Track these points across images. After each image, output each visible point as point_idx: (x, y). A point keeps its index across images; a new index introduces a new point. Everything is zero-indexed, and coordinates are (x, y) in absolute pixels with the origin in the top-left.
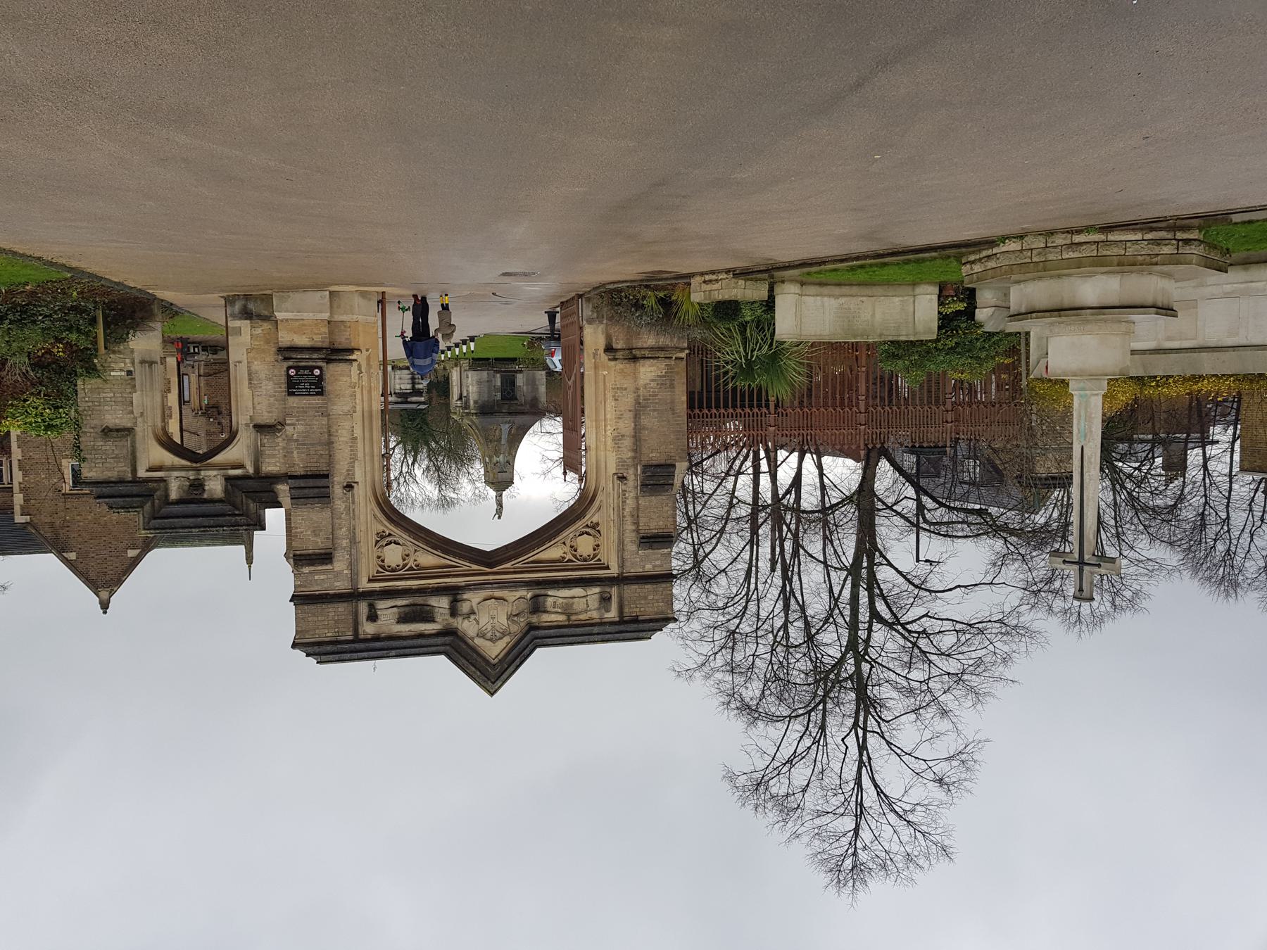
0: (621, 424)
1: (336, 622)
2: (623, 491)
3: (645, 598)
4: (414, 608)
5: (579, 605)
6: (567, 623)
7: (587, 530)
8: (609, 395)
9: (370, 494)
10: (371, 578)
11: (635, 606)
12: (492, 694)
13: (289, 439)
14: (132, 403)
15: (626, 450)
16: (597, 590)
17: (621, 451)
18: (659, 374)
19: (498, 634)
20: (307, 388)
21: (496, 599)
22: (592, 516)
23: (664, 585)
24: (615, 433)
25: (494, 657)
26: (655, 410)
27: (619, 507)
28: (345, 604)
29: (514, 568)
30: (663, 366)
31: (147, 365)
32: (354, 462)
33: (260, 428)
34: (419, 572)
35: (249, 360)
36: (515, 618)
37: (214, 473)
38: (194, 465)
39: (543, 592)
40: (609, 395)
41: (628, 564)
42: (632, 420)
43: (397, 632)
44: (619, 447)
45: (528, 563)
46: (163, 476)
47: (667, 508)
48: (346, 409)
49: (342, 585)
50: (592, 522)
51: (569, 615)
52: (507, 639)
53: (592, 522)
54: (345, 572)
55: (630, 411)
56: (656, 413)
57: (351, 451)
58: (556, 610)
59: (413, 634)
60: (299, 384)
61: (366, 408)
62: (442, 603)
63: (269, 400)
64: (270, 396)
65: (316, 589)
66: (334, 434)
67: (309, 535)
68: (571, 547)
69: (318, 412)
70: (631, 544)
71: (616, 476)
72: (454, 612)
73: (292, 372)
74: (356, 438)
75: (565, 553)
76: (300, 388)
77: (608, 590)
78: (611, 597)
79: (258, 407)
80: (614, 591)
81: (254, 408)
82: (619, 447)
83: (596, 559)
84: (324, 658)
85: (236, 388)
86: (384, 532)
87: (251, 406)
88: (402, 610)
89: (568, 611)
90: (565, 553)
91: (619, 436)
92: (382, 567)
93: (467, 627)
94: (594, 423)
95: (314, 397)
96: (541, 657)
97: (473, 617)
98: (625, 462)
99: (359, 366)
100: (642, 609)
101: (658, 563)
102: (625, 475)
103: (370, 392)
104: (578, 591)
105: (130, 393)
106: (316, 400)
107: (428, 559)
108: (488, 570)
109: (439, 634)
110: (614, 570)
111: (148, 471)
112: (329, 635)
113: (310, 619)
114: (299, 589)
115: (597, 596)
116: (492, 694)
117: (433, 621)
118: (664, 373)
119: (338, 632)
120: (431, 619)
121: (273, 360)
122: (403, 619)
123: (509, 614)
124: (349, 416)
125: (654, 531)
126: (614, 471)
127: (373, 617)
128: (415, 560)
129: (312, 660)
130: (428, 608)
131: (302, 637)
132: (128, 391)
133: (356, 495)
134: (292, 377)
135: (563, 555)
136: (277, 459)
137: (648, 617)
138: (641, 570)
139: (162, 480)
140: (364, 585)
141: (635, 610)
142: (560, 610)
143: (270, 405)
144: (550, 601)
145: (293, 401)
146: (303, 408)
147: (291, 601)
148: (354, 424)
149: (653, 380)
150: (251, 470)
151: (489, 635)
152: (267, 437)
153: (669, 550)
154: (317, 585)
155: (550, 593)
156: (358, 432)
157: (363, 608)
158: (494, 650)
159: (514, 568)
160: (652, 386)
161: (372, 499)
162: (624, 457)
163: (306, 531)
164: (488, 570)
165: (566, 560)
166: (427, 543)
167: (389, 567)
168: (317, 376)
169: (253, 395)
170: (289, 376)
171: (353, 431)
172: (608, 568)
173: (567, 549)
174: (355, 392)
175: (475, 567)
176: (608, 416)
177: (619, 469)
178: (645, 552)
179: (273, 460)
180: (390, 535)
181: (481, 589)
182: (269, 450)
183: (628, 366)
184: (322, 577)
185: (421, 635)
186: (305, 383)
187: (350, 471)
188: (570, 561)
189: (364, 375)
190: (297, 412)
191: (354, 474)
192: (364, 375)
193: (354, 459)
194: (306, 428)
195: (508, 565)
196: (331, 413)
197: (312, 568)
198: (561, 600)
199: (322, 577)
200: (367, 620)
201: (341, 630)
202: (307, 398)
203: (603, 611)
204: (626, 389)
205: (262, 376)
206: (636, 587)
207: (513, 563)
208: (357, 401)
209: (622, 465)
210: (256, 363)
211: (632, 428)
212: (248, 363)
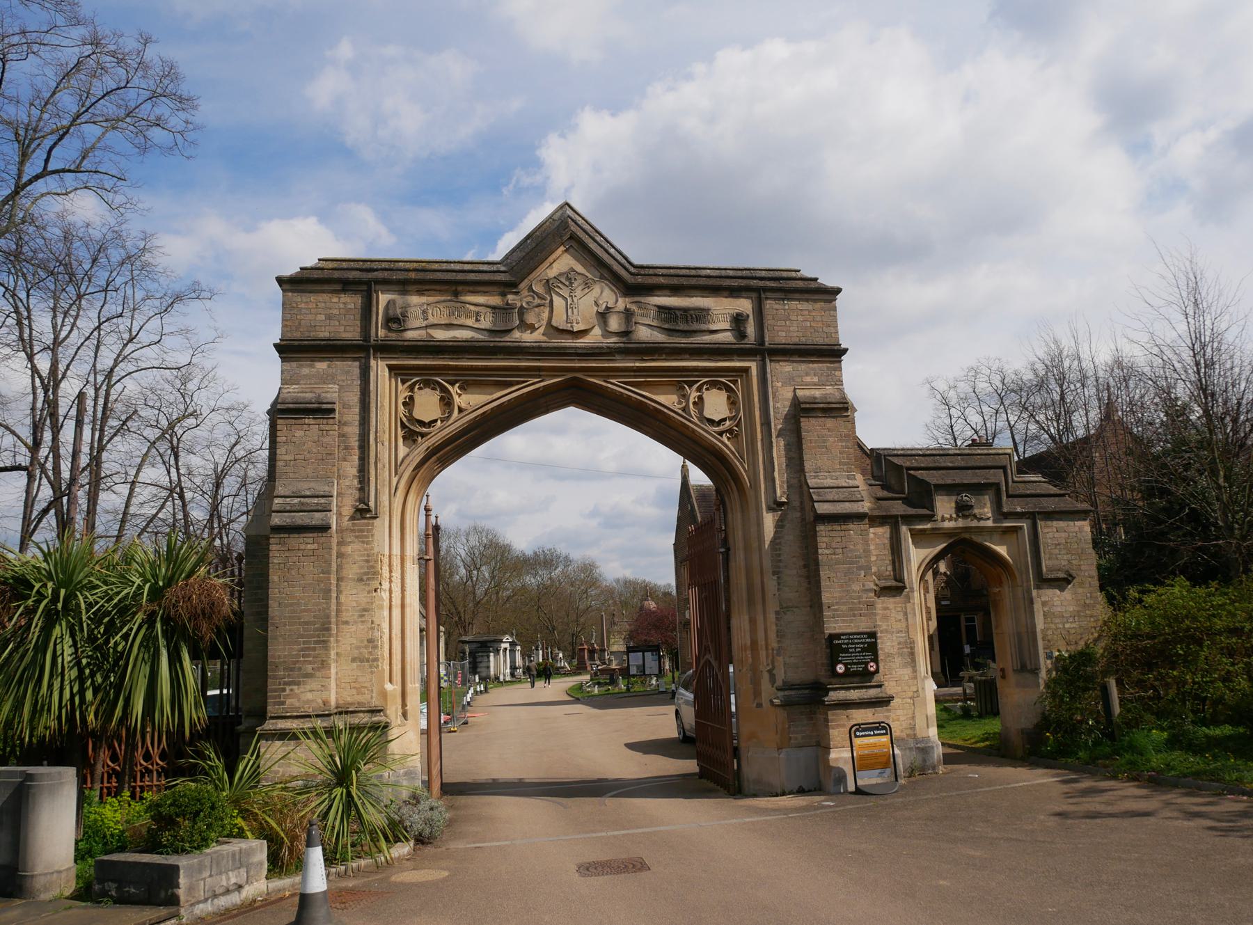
0: (363, 598)
1: (787, 318)
3: (329, 317)
4: (686, 327)
6: (460, 288)
7: (424, 430)
10: (744, 374)
11: (349, 307)
14: (1044, 615)
15: (356, 557)
16: (410, 335)
18: (295, 687)
20: (852, 644)
23: (297, 335)
24: (375, 584)
28: (777, 340)
30: (288, 701)
31: (1029, 668)
34: (680, 380)
37: (947, 524)
44: (368, 561)
47: (287, 458)
54: (779, 384)
55: (347, 623)
57: (779, 555)
58: (477, 309)
60: (864, 650)
62: (644, 334)
63: (888, 626)
64: (887, 631)
67: (831, 436)
69: (835, 610)
70: (351, 404)
74: (774, 573)
76: (862, 643)
77: (390, 334)
79: (901, 616)
80: (380, 333)
81: (906, 614)
82: (368, 561)
84: (794, 274)
88: (704, 327)
91: (368, 579)
93: (607, 295)
95: (841, 631)
97: (602, 309)
98: (357, 537)
101: (305, 371)
103: (754, 643)
105: (1048, 629)
107: (668, 400)
108: (579, 375)
109: (650, 290)
113: (820, 325)
114: (836, 365)
117: (660, 307)
118: (288, 688)
120: (661, 308)
122: (701, 314)
124: (785, 605)
125: (312, 421)
126: (376, 522)
127: (738, 321)
132: (1050, 632)
134: (872, 660)
142: (472, 308)
143: (885, 618)
147: (845, 351)
150: (904, 529)
152: (888, 573)
154: (813, 369)
156: (771, 583)
158: (562, 262)
160: (310, 667)
164: (579, 375)
165: (457, 385)
168: (840, 662)
169: (908, 632)
170: (876, 660)
171: (779, 584)
174: (779, 642)
177: (368, 525)
180: (721, 434)
183: (349, 699)
184: (808, 379)
185: (676, 290)
192: (764, 667)
194: (850, 586)
196: (809, 608)
198: (470, 322)
199: (808, 379)
200: (748, 316)
201: (780, 307)
204: (354, 660)
205: (898, 660)
208: (774, 628)
209: (362, 531)
210: (907, 677)
211: (344, 593)
212: (915, 678)
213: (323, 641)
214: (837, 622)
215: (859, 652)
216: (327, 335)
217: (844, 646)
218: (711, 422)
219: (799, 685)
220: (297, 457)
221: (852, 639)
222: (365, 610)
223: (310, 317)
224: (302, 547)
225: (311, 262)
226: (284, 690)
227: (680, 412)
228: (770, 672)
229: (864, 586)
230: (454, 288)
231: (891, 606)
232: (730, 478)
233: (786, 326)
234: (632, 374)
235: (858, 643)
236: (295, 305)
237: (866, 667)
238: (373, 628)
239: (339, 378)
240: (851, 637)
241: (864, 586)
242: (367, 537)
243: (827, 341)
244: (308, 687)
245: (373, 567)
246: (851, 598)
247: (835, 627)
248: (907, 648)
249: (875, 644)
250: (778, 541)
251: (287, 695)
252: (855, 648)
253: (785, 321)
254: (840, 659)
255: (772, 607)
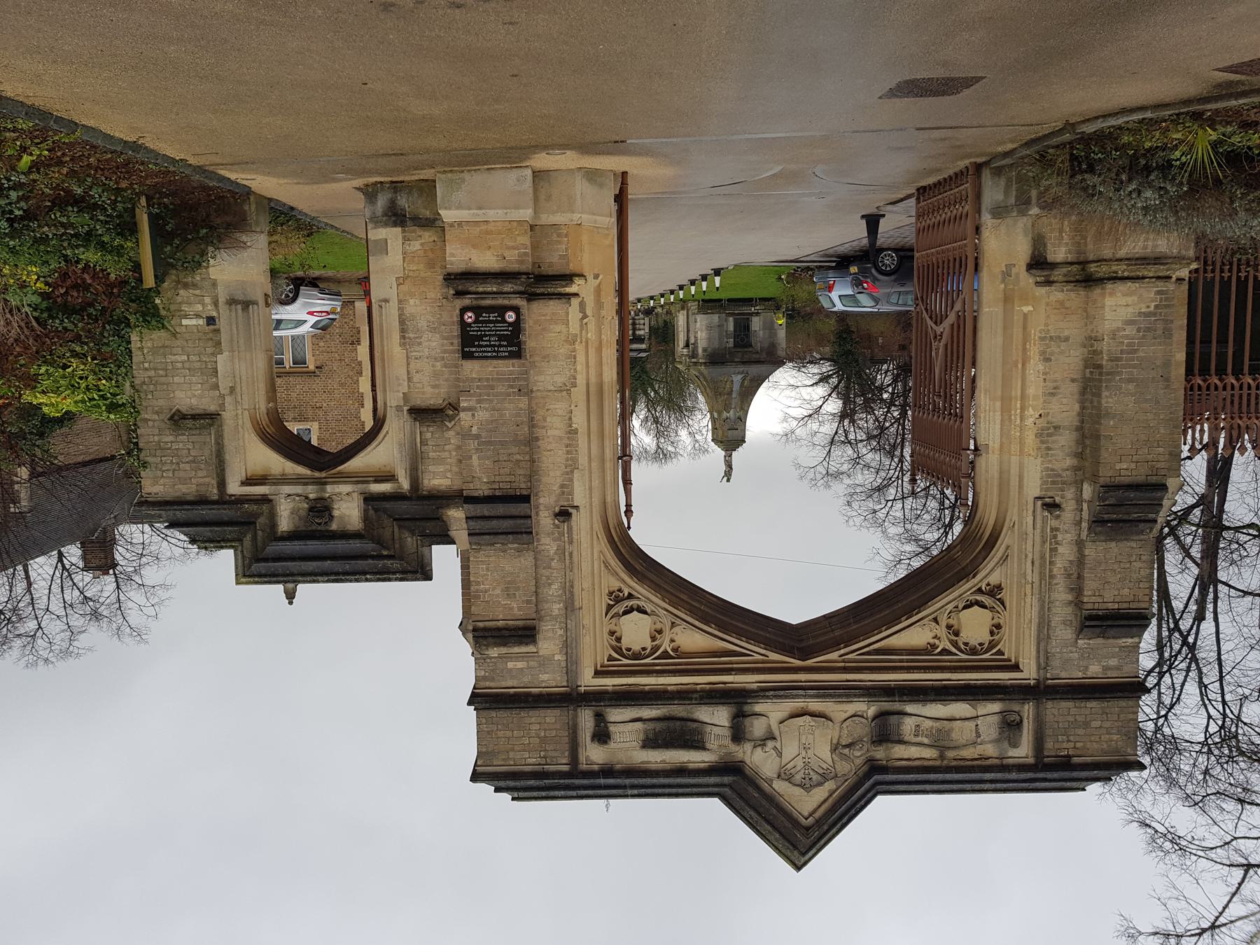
1: (543, 740)
2: (1052, 530)
3: (1086, 724)
4: (671, 724)
5: (961, 733)
6: (938, 763)
7: (979, 598)
8: (1034, 351)
9: (598, 527)
10: (599, 668)
12: (798, 868)
13: (465, 435)
14: (217, 372)
15: (1061, 454)
16: (995, 707)
17: (1052, 455)
19: (815, 777)
21: (813, 715)
22: (990, 573)
23: (1123, 703)
24: (1042, 423)
25: (806, 814)
26: (1130, 381)
27: (1042, 557)
28: (557, 712)
29: (843, 661)
31: (239, 307)
32: (572, 472)
33: (421, 414)
34: (680, 661)
35: (401, 296)
36: (846, 751)
37: (345, 488)
38: (317, 474)
39: (897, 706)
40: (1034, 351)
41: (1056, 662)
42: (1076, 397)
43: (642, 763)
44: (1048, 449)
45: (868, 653)
46: (267, 492)
47: (1138, 565)
48: (560, 380)
49: (551, 680)
50: (988, 585)
51: (942, 749)
52: (830, 785)
53: (988, 585)
55: (1073, 380)
56: (1131, 386)
57: (568, 452)
58: (919, 739)
59: (668, 767)
60: (480, 338)
61: (593, 380)
62: (717, 718)
63: (433, 366)
65: (510, 684)
66: (540, 424)
67: (497, 596)
68: (949, 627)
69: (511, 387)
70: (1062, 627)
71: (1039, 503)
72: (738, 735)
73: (469, 317)
74: (576, 432)
75: (935, 637)
78: (1021, 721)
81: (409, 379)
82: (1048, 449)
83: (994, 651)
84: (521, 794)
85: (382, 346)
86: (620, 590)
87: (406, 378)
88: (650, 726)
89: (940, 741)
90: (935, 637)
91: (1049, 429)
92: (618, 650)
93: (761, 761)
94: (998, 404)
95: (506, 361)
96: (883, 805)
98: (1060, 476)
99: (582, 306)
100: (1079, 745)
101: (1113, 662)
102: (1058, 500)
103: (599, 349)
104: (960, 708)
105: (213, 354)
106: (507, 367)
107: (693, 639)
109: (711, 770)
110: (1029, 672)
111: (243, 484)
112: (529, 761)
113: (500, 734)
114: (482, 684)
115: (996, 718)
116: (798, 868)
117: (704, 748)
118: (1152, 308)
119: (545, 757)
121: (439, 295)
122: (651, 742)
123: (835, 741)
125: (1110, 606)
126: (1037, 493)
128: (672, 641)
129: (506, 797)
130: (695, 725)
131: (489, 763)
132: (209, 350)
133: (575, 528)
134: (469, 325)
135: (932, 641)
136: (448, 467)
137: (1089, 759)
138: (1080, 675)
139: (265, 500)
140: (588, 680)
141: (1065, 745)
142: (926, 741)
143: (436, 375)
144: (908, 724)
145: (472, 368)
146: (488, 379)
148: (573, 407)
149: (1130, 322)
150: (405, 485)
151: (798, 778)
152: (431, 429)
153: (1136, 640)
154: (512, 677)
155: (909, 708)
156: (579, 421)
157: (586, 719)
159: (843, 661)
161: (603, 536)
162: (1057, 466)
163: (493, 590)
165: (939, 650)
166: (692, 611)
167: (629, 650)
168: (510, 324)
171: (570, 419)
172: (1016, 668)
173: (942, 631)
175: (774, 656)
176: (1031, 391)
178: (1091, 642)
179: (441, 468)
180: (630, 596)
181: (786, 697)
182: (434, 451)
183: (1073, 295)
185: (681, 771)
186: (490, 335)
187: (566, 488)
188: (945, 652)
189: (591, 322)
190: (478, 387)
191: (571, 493)
192: (591, 322)
193: (572, 466)
194: (492, 415)
195: (834, 656)
196: (535, 389)
197: (504, 650)
198: (929, 723)
199: (520, 665)
200: (593, 740)
201: (550, 754)
202: (495, 362)
203: (1006, 744)
204: (1067, 339)
205: (423, 324)
206: (1070, 704)
207: (842, 651)
208: (579, 368)
209: (1053, 483)
210: (412, 302)
211: (1075, 413)
212: (400, 302)
213: (1112, 361)
214: (511, 373)
215: (486, 336)
216: (1089, 704)
217: (505, 343)
218: (642, 611)
219: (551, 299)
220: (1128, 565)
221: (494, 351)
222: (1053, 394)
223: (1107, 724)
224: (1133, 466)
225: (1094, 788)
226: (1156, 307)
227: (678, 621)
228: (585, 316)
229: (473, 415)
230: (945, 762)
231: (428, 390)
232: (618, 544)
233: (545, 730)
234: (735, 666)
235: (486, 346)
236: (1124, 738)
237: (477, 318)
238: (1044, 374)
239: (1076, 655)
240: (494, 354)
241: (473, 415)
242: (1049, 476)
243: (493, 714)
244: (1130, 310)
245: (1042, 442)
246: (491, 401)
247: (513, 366)
248: (409, 338)
249: (463, 346)
250: (568, 470)
251: (1152, 301)
252: (489, 341)
253: (545, 737)
254: (510, 328)
255: (579, 393)
